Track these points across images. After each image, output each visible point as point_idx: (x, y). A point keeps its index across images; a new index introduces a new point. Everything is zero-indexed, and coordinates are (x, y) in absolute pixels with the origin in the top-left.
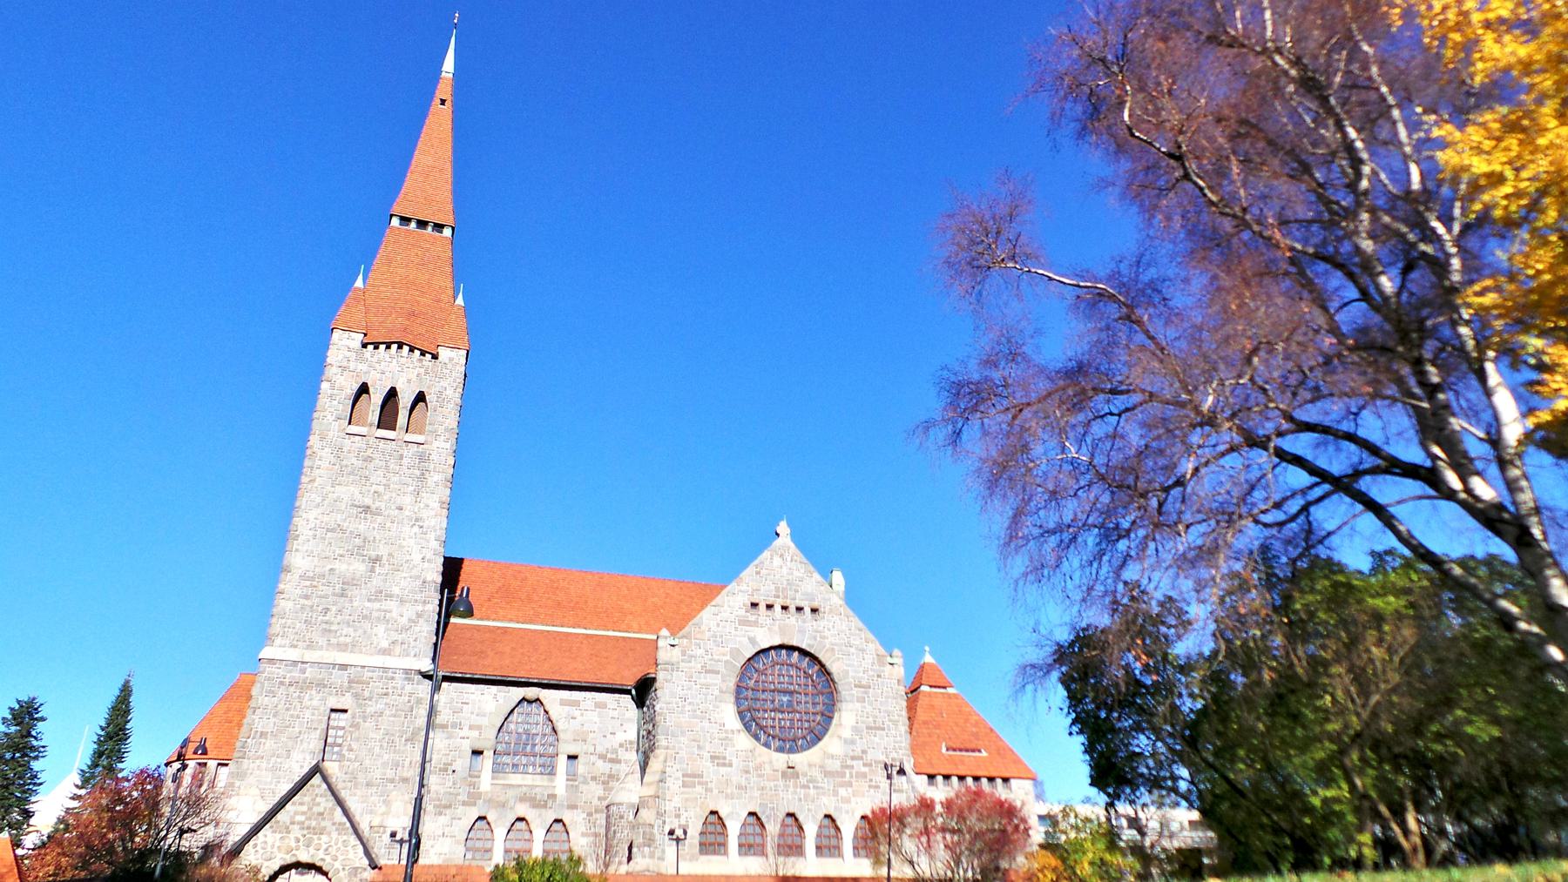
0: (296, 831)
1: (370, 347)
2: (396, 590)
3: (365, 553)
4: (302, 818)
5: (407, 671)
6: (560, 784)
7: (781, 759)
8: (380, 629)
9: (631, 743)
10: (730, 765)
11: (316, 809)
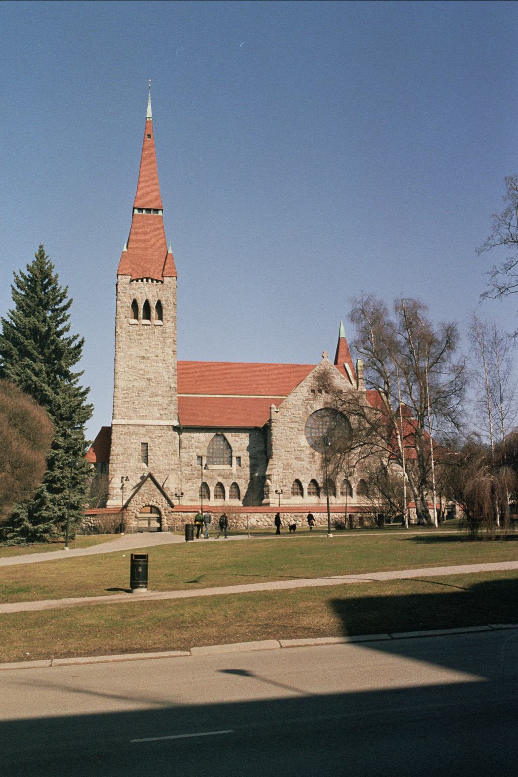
1: (135, 282)
3: (145, 377)
4: (147, 491)
8: (156, 409)
10: (303, 461)
11: (152, 488)
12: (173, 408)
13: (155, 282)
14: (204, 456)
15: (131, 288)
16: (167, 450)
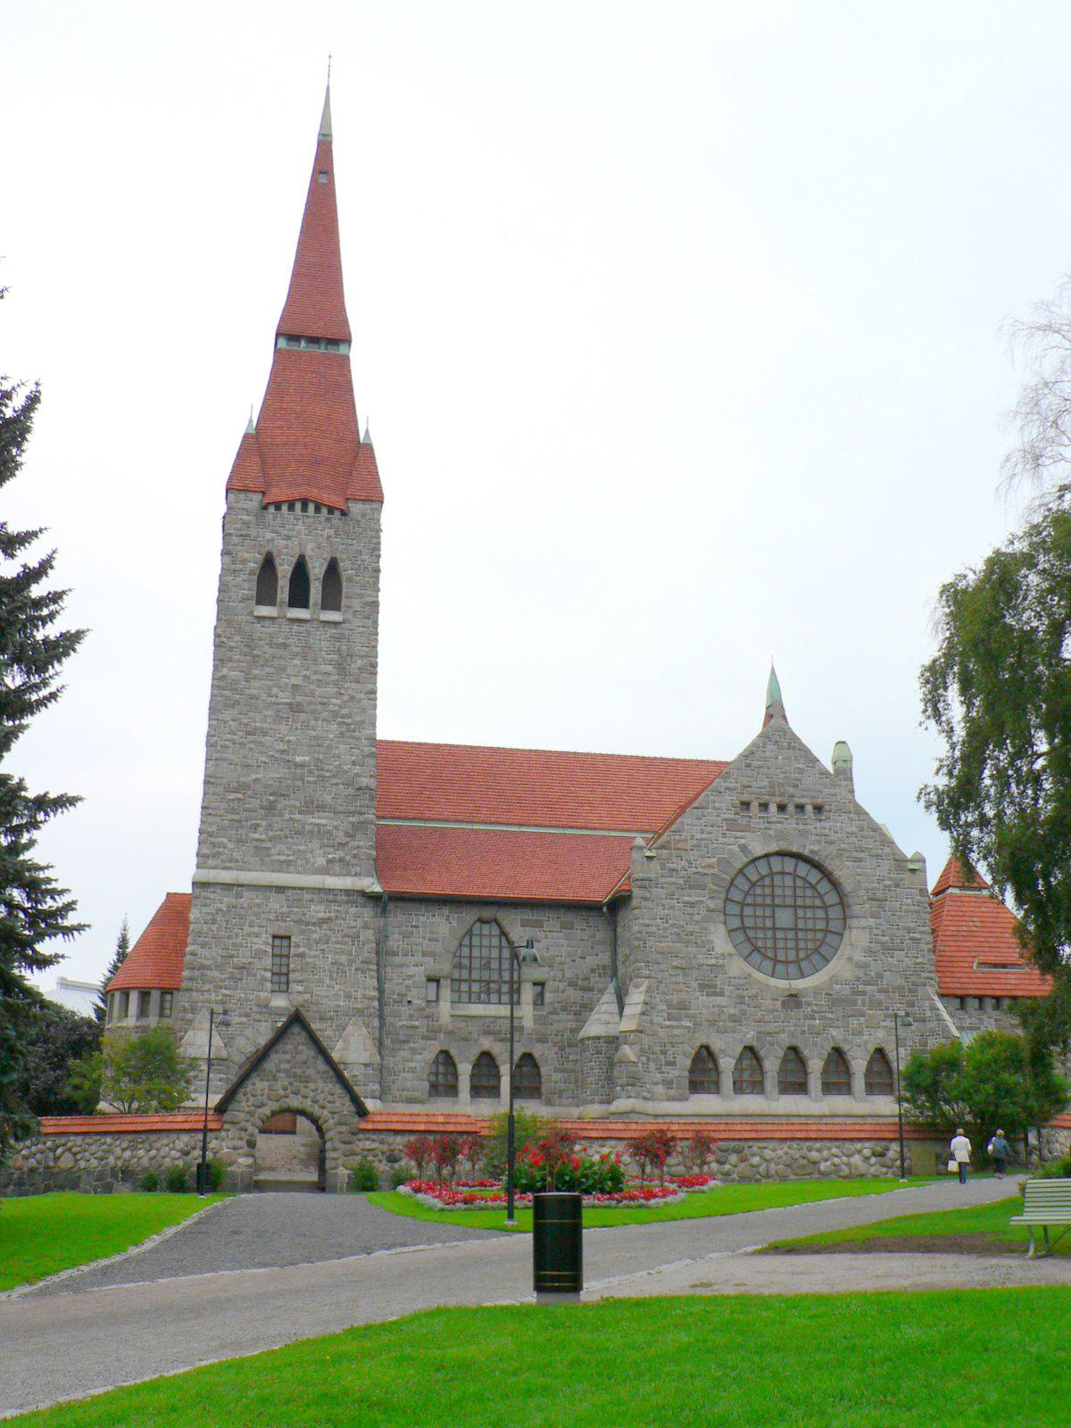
0: (283, 1081)
1: (272, 509)
2: (328, 799)
4: (287, 1066)
5: (348, 892)
6: (526, 1012)
7: (783, 984)
9: (604, 967)
10: (722, 995)
11: (299, 1058)
12: (364, 844)
13: (324, 510)
14: (446, 977)
15: (260, 521)
16: (343, 959)
